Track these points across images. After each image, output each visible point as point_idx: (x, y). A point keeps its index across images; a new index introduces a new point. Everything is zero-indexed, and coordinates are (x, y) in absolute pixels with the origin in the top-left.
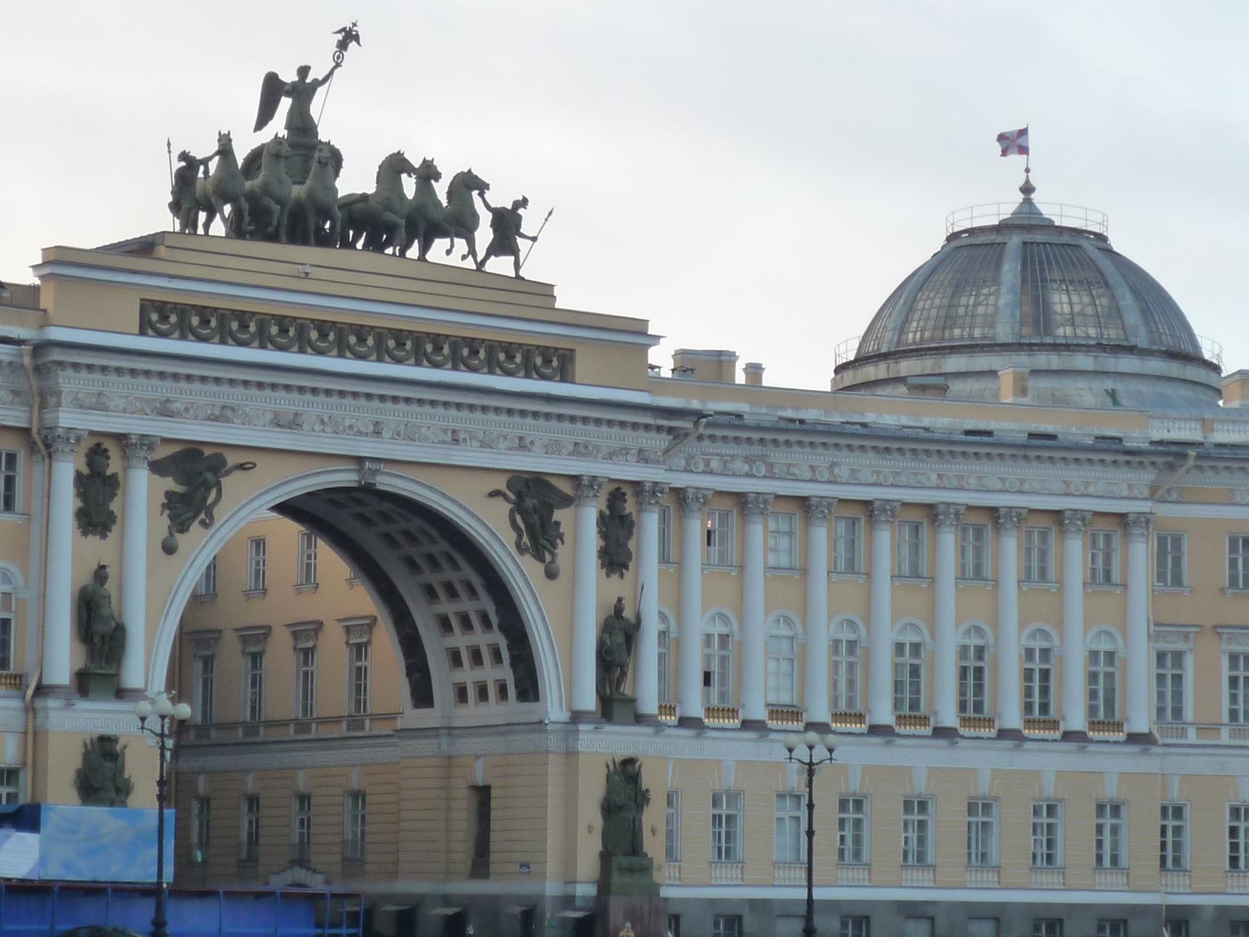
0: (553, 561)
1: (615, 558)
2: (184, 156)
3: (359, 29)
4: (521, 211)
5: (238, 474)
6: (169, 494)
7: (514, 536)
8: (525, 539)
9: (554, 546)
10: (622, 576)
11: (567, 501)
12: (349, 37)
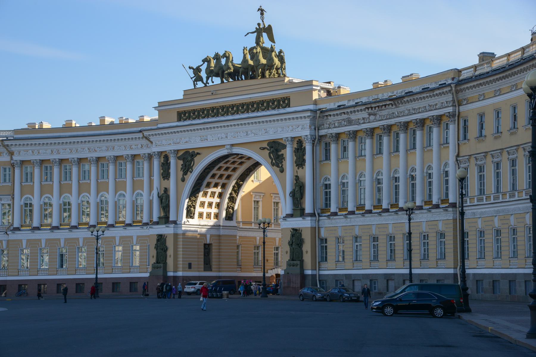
0: (282, 167)
1: (300, 163)
2: (190, 68)
3: (263, 8)
4: (282, 54)
5: (198, 156)
6: (182, 165)
7: (270, 161)
8: (274, 161)
9: (282, 162)
10: (303, 168)
11: (284, 147)
12: (262, 11)
